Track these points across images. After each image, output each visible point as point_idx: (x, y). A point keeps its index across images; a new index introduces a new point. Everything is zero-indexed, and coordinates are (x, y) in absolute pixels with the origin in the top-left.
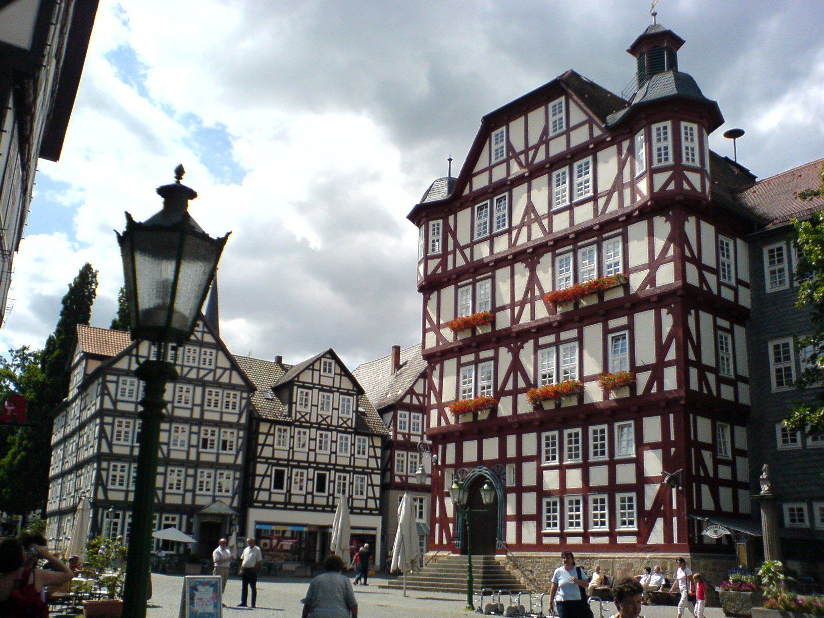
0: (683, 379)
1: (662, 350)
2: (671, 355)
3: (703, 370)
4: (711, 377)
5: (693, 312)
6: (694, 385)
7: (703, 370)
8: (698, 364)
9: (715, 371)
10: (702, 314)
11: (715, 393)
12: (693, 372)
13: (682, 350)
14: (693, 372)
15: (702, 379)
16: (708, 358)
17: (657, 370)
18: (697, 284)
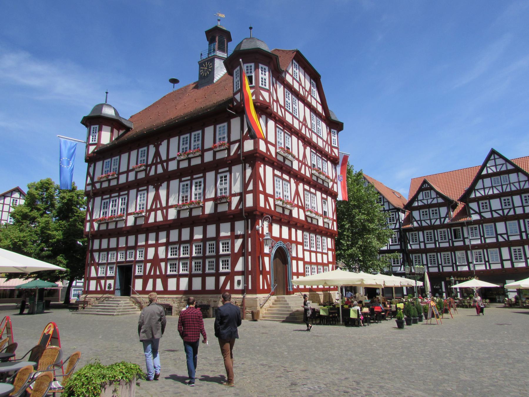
0: (256, 200)
1: (245, 185)
2: (250, 187)
3: (267, 196)
4: (271, 200)
5: (262, 165)
6: (262, 204)
7: (267, 196)
8: (264, 192)
9: (273, 196)
10: (267, 167)
11: (273, 209)
12: (262, 197)
13: (256, 186)
14: (262, 197)
15: (266, 200)
16: (269, 191)
17: (242, 196)
18: (265, 151)
